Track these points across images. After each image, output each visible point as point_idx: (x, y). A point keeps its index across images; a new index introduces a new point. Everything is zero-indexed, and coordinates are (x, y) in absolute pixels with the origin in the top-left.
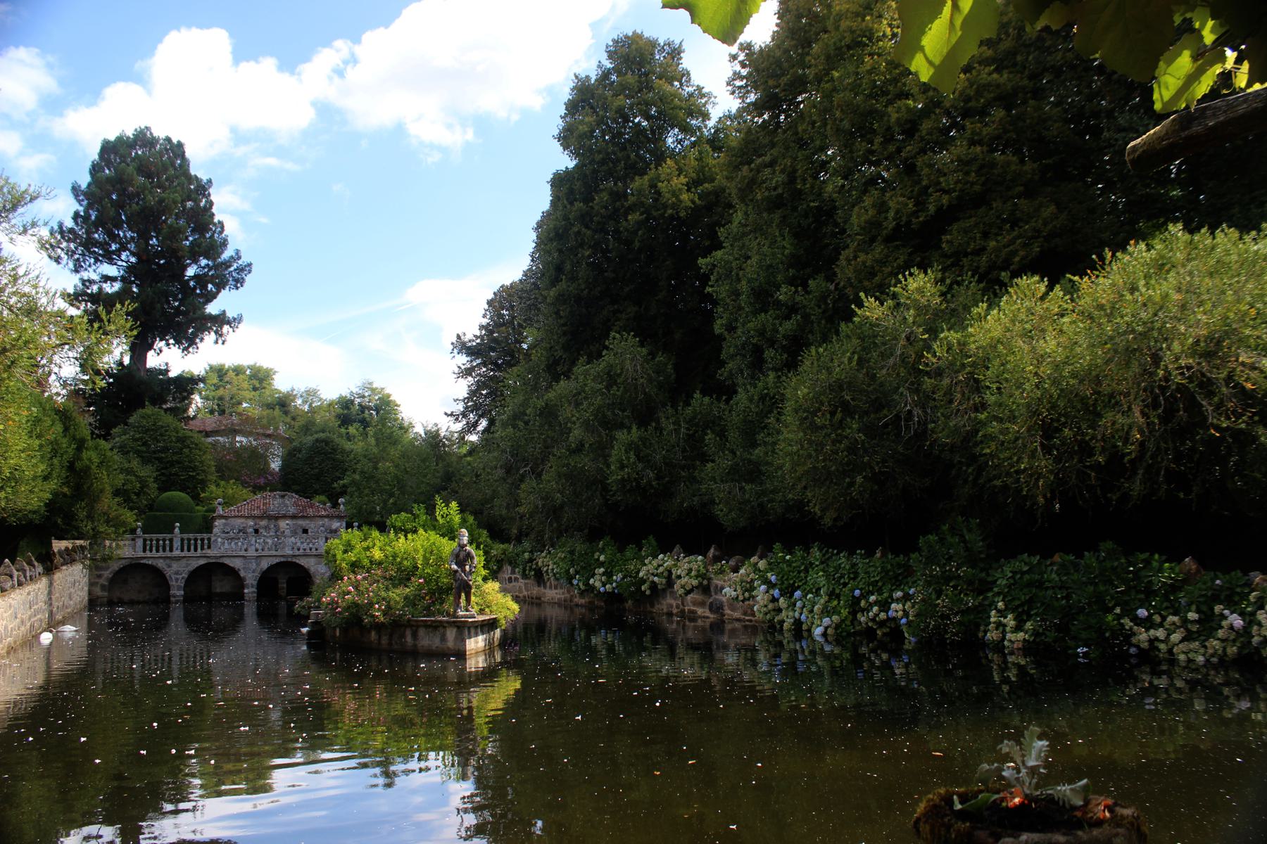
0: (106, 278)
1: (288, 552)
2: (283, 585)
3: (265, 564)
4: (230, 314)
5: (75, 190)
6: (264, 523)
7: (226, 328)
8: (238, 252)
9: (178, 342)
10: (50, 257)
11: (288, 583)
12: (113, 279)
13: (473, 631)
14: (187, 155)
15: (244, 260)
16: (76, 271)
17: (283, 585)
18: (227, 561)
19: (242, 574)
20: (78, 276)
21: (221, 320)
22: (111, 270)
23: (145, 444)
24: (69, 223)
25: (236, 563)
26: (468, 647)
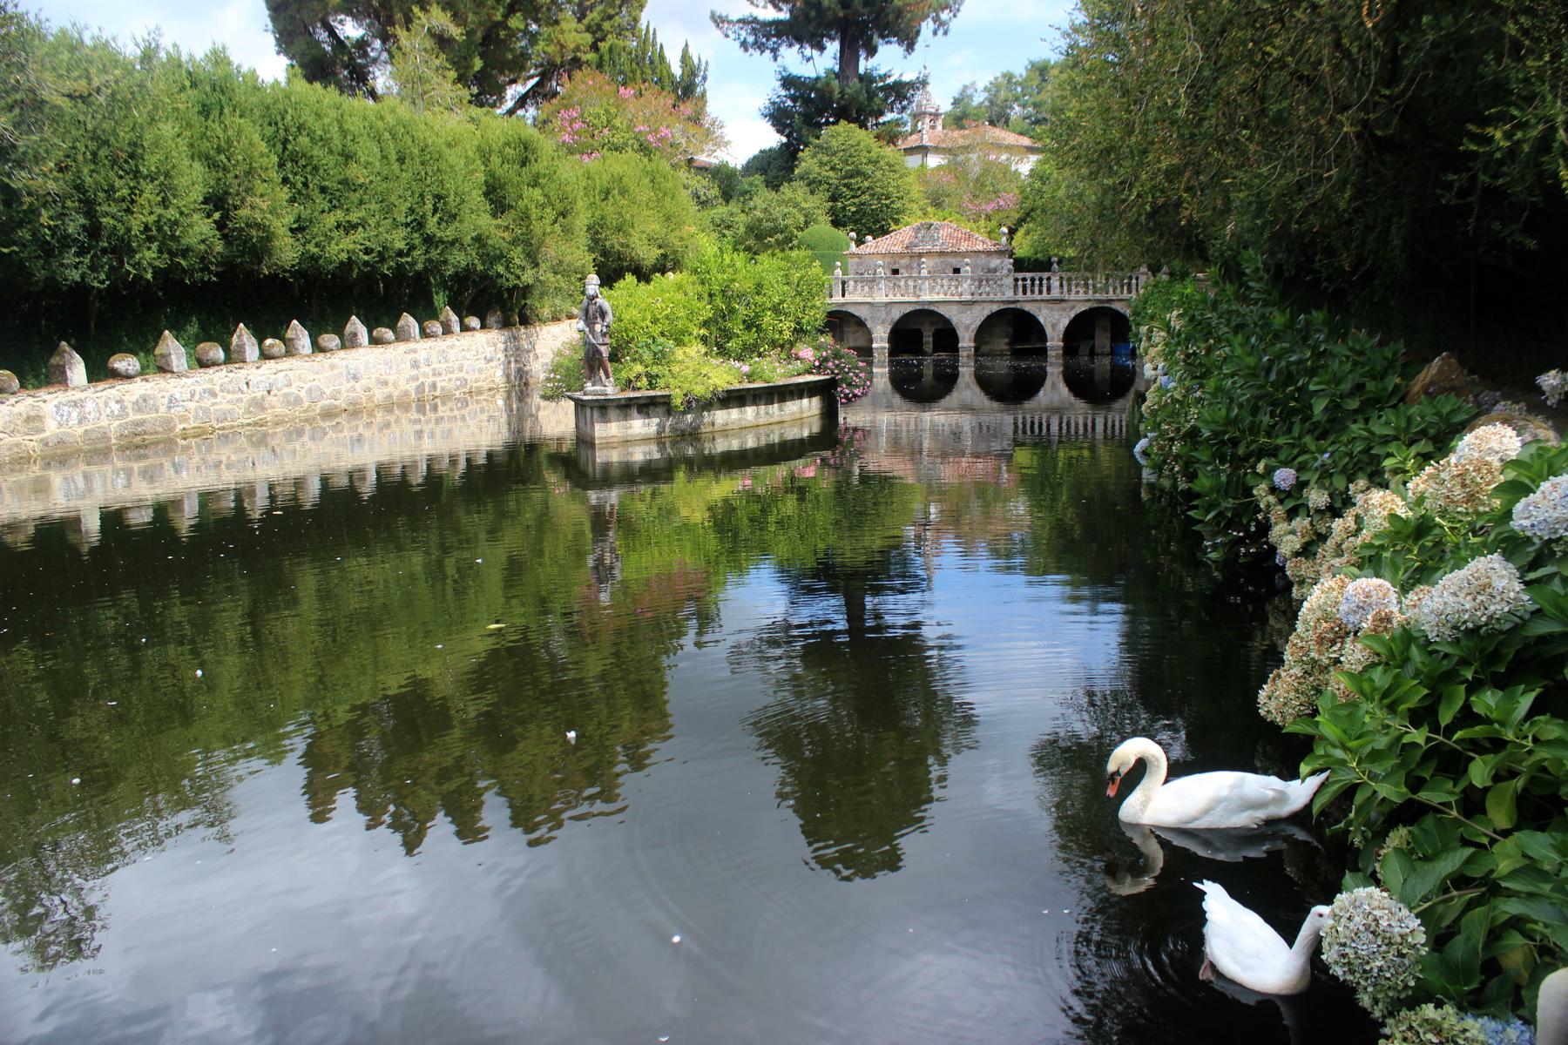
1: (927, 298)
2: (928, 340)
3: (896, 314)
6: (904, 261)
7: (944, 16)
9: (900, 43)
11: (934, 336)
13: (612, 413)
17: (928, 340)
18: (851, 310)
23: (833, 169)
26: (597, 434)
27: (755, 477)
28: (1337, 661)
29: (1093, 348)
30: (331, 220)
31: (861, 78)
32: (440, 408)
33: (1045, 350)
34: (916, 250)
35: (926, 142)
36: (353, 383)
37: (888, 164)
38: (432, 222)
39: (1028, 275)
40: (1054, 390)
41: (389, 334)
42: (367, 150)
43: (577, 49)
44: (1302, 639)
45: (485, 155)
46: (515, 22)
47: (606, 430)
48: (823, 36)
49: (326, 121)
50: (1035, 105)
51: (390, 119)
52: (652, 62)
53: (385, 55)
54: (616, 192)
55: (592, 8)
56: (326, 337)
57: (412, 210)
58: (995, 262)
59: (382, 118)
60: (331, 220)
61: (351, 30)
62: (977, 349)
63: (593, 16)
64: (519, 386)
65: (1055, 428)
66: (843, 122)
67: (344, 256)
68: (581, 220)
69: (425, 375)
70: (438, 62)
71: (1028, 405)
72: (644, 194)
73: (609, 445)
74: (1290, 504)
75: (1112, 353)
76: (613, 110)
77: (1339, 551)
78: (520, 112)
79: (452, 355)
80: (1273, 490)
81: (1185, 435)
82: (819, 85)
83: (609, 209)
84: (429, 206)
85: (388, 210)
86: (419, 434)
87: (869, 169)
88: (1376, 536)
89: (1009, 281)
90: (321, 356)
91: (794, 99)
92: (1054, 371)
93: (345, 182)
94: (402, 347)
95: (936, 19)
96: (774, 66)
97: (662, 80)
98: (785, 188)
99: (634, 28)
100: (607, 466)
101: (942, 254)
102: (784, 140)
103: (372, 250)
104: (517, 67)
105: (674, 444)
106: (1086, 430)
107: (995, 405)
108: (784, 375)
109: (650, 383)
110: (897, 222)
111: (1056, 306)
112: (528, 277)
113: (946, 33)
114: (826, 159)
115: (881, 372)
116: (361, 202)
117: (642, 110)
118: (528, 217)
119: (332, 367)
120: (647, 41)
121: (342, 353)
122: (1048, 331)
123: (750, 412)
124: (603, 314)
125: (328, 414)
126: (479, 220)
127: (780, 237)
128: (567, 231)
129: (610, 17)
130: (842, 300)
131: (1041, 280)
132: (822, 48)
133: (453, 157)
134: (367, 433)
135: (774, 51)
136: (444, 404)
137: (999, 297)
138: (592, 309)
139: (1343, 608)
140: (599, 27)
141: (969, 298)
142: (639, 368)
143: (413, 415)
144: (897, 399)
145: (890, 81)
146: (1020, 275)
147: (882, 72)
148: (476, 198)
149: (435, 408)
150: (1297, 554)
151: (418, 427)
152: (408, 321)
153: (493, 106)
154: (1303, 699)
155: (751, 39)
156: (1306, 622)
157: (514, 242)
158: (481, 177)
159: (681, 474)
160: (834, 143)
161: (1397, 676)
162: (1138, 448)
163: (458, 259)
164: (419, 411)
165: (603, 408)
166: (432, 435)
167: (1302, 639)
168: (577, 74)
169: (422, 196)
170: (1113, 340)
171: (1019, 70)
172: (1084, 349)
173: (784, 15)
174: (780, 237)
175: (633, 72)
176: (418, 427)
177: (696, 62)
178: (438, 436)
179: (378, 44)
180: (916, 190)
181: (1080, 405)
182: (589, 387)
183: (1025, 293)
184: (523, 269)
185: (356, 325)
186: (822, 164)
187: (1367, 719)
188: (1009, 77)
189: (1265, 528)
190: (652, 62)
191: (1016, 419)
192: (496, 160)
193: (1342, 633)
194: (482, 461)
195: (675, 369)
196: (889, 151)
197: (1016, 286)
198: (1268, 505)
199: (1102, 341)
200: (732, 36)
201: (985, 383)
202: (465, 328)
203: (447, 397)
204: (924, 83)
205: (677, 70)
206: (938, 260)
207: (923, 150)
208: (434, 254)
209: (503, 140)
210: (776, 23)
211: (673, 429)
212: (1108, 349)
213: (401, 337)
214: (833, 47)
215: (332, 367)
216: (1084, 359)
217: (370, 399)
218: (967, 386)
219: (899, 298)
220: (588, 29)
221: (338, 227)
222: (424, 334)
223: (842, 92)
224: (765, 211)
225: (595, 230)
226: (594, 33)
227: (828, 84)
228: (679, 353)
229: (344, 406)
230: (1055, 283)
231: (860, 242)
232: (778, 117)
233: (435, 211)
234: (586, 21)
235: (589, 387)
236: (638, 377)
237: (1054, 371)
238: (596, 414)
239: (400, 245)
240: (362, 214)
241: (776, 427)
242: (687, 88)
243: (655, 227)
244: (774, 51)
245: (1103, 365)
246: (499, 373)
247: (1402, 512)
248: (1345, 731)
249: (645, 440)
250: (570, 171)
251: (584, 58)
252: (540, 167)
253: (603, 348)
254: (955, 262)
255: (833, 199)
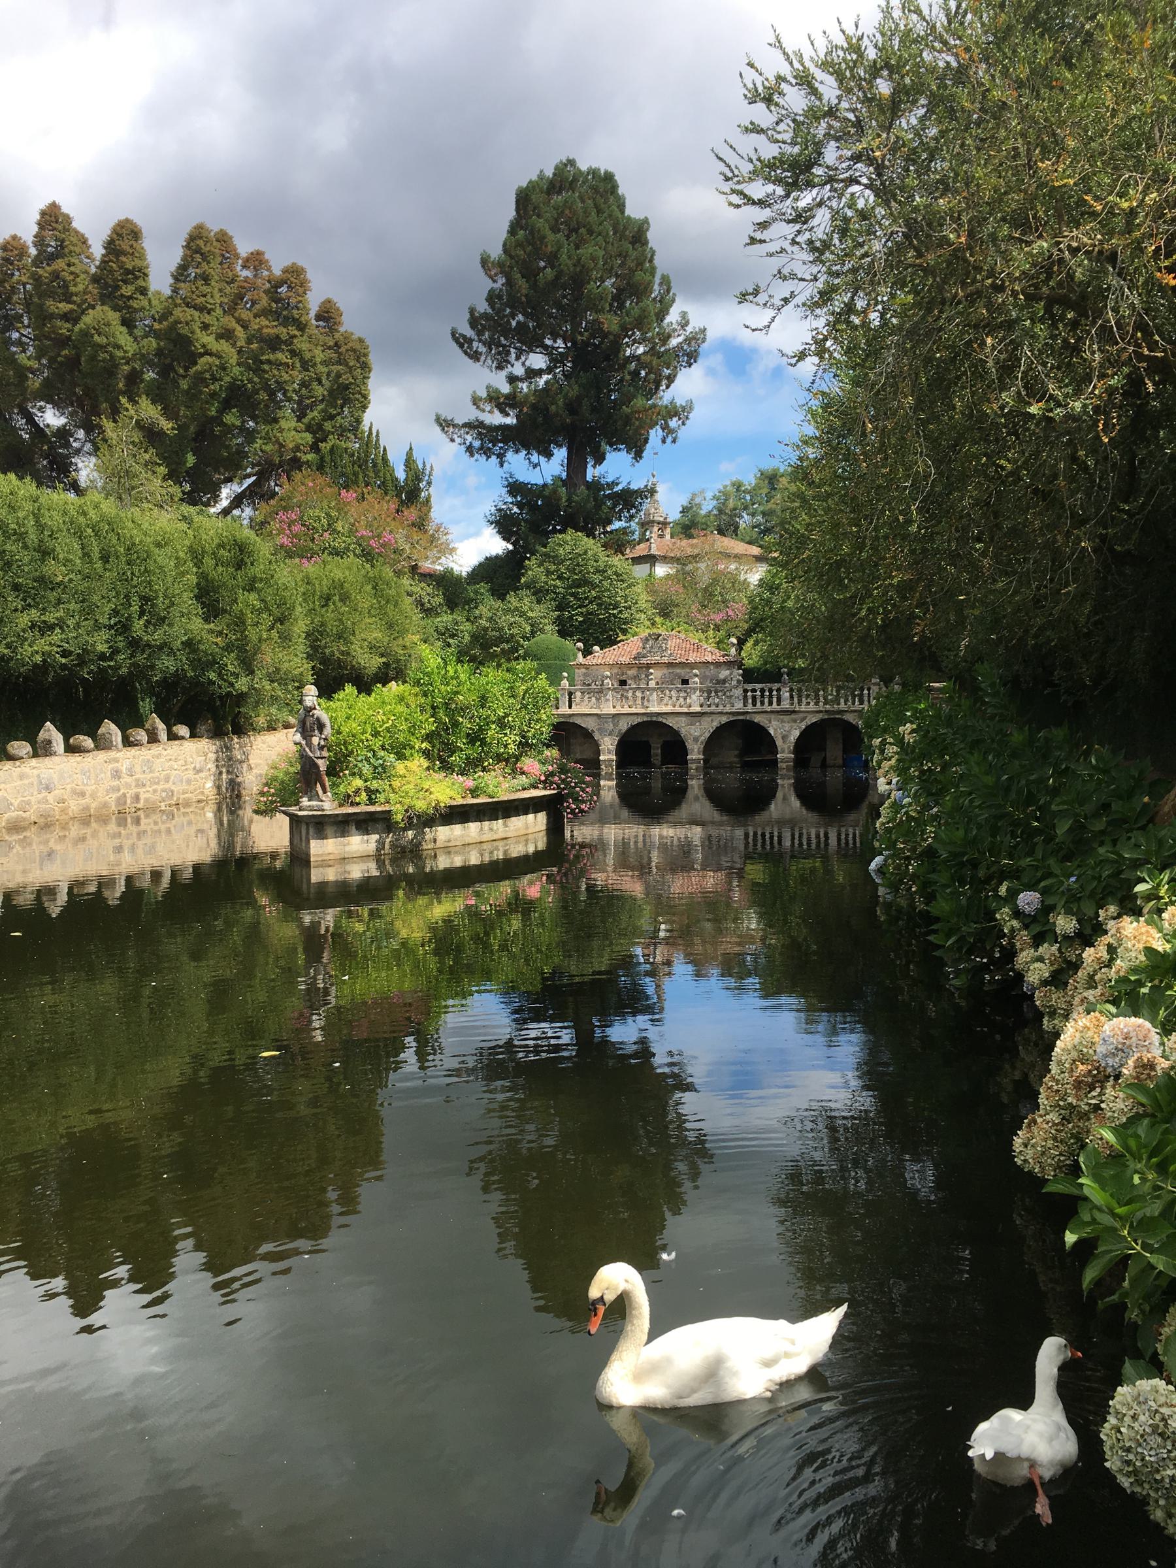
0: (532, 374)
1: (654, 709)
2: (656, 751)
3: (624, 726)
4: (680, 402)
5: (484, 262)
6: (630, 673)
7: (673, 423)
8: (684, 315)
10: (466, 353)
12: (540, 372)
13: (329, 830)
14: (620, 192)
15: (694, 325)
16: (500, 367)
17: (656, 751)
18: (578, 721)
19: (597, 736)
20: (503, 374)
21: (674, 411)
22: (538, 361)
23: (560, 578)
24: (483, 307)
25: (589, 724)
26: (313, 851)
27: (478, 894)
28: (1097, 1108)
29: (824, 760)
30: (24, 620)
31: (589, 486)
32: (143, 821)
33: (775, 762)
34: (644, 661)
35: (654, 551)
36: (44, 794)
37: (616, 573)
38: (138, 625)
39: (758, 686)
40: (786, 803)
41: (88, 742)
42: (67, 547)
43: (297, 448)
44: (1057, 1082)
45: (197, 555)
46: (231, 418)
47: (321, 848)
48: (550, 442)
49: (21, 514)
50: (764, 514)
51: (92, 514)
52: (375, 465)
53: (88, 447)
54: (337, 598)
55: (311, 407)
56: (16, 743)
57: (116, 612)
58: (724, 673)
59: (85, 514)
60: (24, 620)
61: (52, 418)
62: (706, 761)
63: (314, 415)
64: (230, 797)
65: (787, 843)
66: (570, 531)
67: (38, 658)
68: (300, 627)
69: (128, 786)
70: (147, 456)
71: (759, 818)
72: (365, 601)
73: (325, 864)
74: (1037, 929)
75: (844, 765)
76: (334, 514)
77: (1091, 983)
78: (236, 512)
79: (158, 765)
80: (1017, 914)
81: (921, 855)
82: (546, 493)
83: (330, 615)
84: (135, 608)
85: (88, 611)
86: (119, 849)
87: (596, 578)
88: (1134, 970)
89: (739, 692)
90: (8, 765)
91: (520, 505)
92: (785, 784)
93: (42, 580)
94: (102, 756)
95: (665, 427)
96: (500, 472)
97: (387, 484)
98: (512, 600)
99: (356, 429)
100: (323, 885)
101: (670, 665)
102: (511, 547)
103: (71, 653)
104: (232, 467)
105: (394, 861)
106: (818, 843)
107: (725, 818)
108: (508, 790)
109: (370, 799)
110: (625, 632)
111: (786, 718)
112: (242, 684)
113: (674, 441)
114: (553, 567)
115: (609, 788)
116: (59, 602)
117: (365, 513)
118: (243, 623)
119: (22, 777)
120: (370, 443)
121: (34, 762)
122: (779, 743)
123: (473, 827)
124: (321, 727)
125: (15, 827)
126: (190, 623)
127: (506, 646)
128: (285, 638)
129: (332, 417)
130: (569, 712)
131: (771, 691)
132: (549, 455)
133: (161, 557)
134: (58, 848)
135: (501, 456)
136: (147, 816)
137: (728, 709)
138: (309, 721)
139: (1101, 1049)
140: (320, 427)
141: (698, 709)
142: (358, 783)
143: (112, 827)
144: (625, 813)
145: (620, 487)
146: (750, 687)
147: (610, 480)
148: (187, 600)
149: (137, 821)
150: (1045, 983)
151: (117, 841)
152: (110, 728)
153: (207, 505)
154: (1062, 1148)
155: (477, 444)
156: (1060, 1063)
157: (228, 648)
158: (193, 579)
159: (401, 893)
160: (561, 551)
161: (1166, 1132)
162: (873, 866)
163: (168, 664)
164: (119, 825)
165: (321, 825)
166: (133, 848)
167: (1057, 1082)
168: (297, 476)
169: (127, 597)
170: (844, 751)
171: (749, 479)
172: (815, 760)
173: (511, 420)
174: (506, 646)
175: (355, 474)
176: (117, 841)
177: (420, 466)
178: (140, 851)
179: (81, 434)
180: (643, 599)
181: (812, 817)
182: (305, 802)
183: (754, 704)
184: (237, 676)
185: (50, 732)
186: (548, 573)
187: (1136, 1180)
188: (738, 486)
189: (1010, 954)
190: (375, 465)
191: (747, 835)
192: (209, 562)
193: (1101, 1077)
194: (187, 874)
195: (396, 783)
196: (616, 560)
197: (745, 698)
198: (1013, 930)
199: (834, 752)
200: (458, 440)
201: (714, 796)
202: (172, 737)
203: (151, 810)
204: (653, 491)
205: (401, 474)
206: (666, 671)
207: (651, 559)
208: (140, 658)
209: (216, 541)
210: (503, 428)
211: (393, 846)
212: (840, 761)
213: (102, 744)
214: (560, 454)
215: (22, 777)
216: (815, 772)
217: (63, 811)
218: (697, 798)
219: (626, 710)
220: (309, 428)
221: (33, 626)
222: (128, 742)
223: (569, 500)
224: (491, 619)
225: (314, 637)
226: (314, 433)
227: (555, 491)
228: (400, 767)
229: (33, 819)
230: (786, 695)
231: (587, 652)
232: (504, 524)
233: (142, 613)
234: (305, 420)
235: (305, 802)
236: (357, 792)
237: (785, 784)
238: (311, 831)
239: (102, 648)
240: (61, 614)
241: (501, 844)
242: (411, 493)
243: (376, 635)
244: (501, 456)
245: (834, 778)
246: (209, 784)
247: (1161, 946)
248: (1112, 1195)
249: (364, 858)
250: (287, 574)
251: (304, 458)
252: (257, 570)
253: (320, 762)
254: (681, 672)
255: (560, 608)
